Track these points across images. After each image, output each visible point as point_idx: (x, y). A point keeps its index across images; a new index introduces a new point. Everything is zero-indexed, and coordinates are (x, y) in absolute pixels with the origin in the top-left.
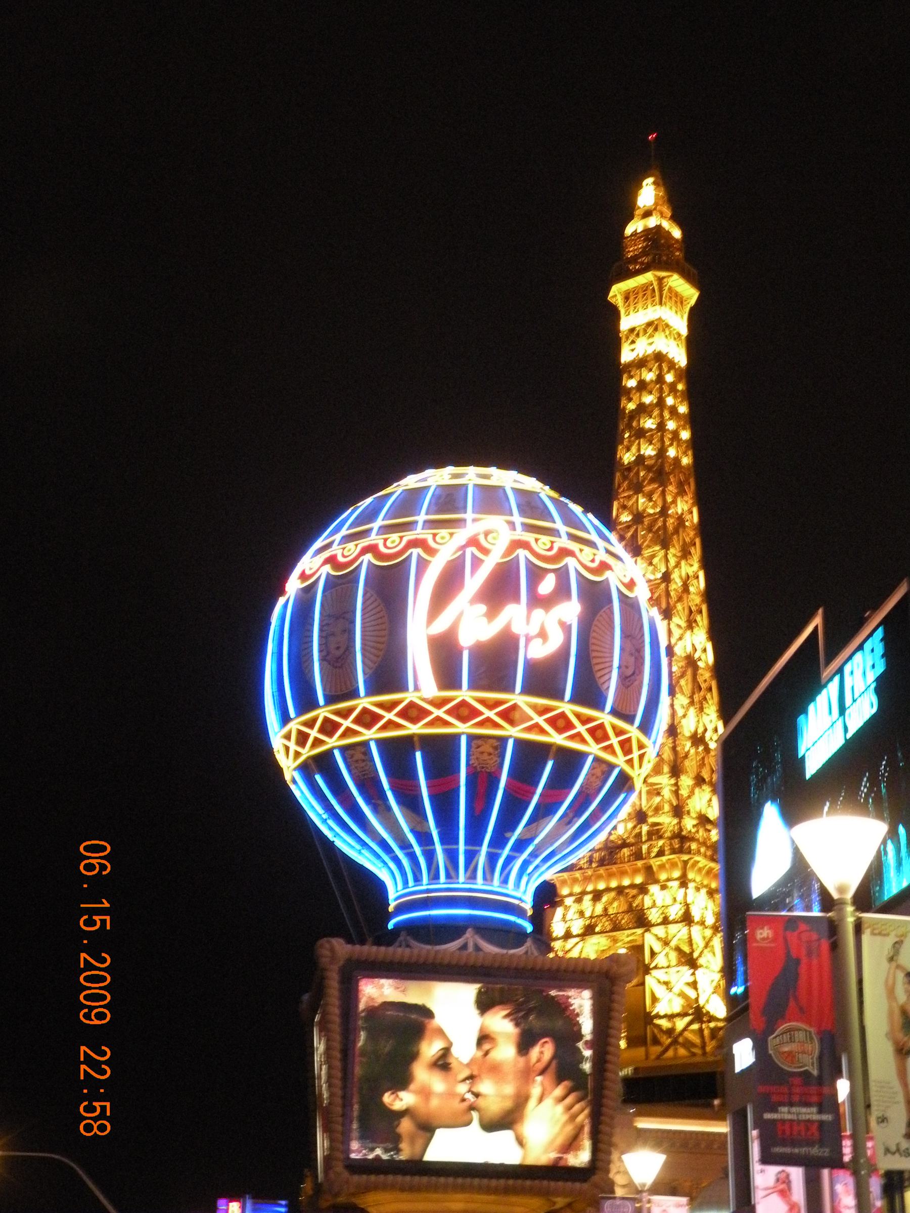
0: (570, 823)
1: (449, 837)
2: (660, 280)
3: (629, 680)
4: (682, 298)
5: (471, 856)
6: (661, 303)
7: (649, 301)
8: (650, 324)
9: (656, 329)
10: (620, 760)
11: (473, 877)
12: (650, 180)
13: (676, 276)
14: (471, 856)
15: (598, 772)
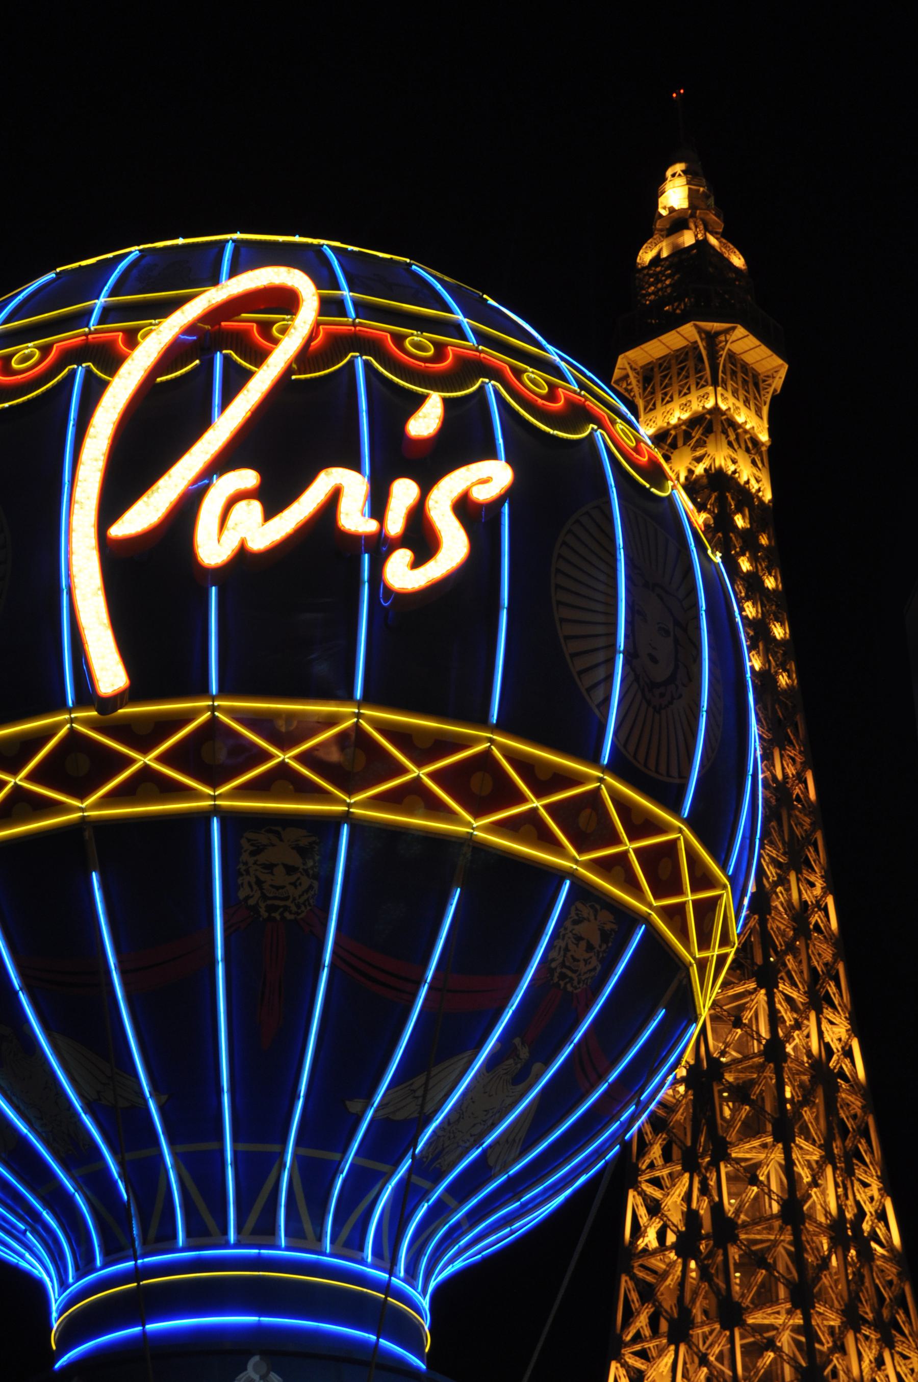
0: (523, 1079)
1: (193, 1120)
2: (711, 339)
3: (661, 690)
4: (756, 375)
5: (257, 1171)
6: (715, 384)
7: (692, 382)
8: (696, 421)
9: (709, 430)
10: (648, 905)
11: (264, 1231)
12: (679, 167)
13: (740, 331)
14: (257, 1171)
15: (590, 930)
